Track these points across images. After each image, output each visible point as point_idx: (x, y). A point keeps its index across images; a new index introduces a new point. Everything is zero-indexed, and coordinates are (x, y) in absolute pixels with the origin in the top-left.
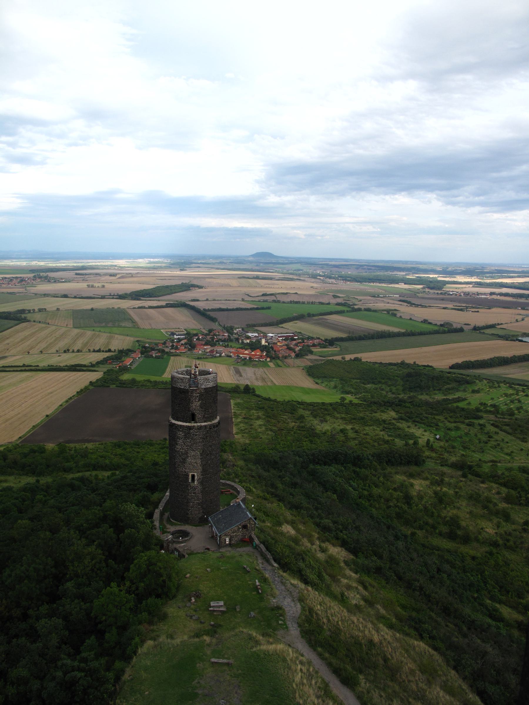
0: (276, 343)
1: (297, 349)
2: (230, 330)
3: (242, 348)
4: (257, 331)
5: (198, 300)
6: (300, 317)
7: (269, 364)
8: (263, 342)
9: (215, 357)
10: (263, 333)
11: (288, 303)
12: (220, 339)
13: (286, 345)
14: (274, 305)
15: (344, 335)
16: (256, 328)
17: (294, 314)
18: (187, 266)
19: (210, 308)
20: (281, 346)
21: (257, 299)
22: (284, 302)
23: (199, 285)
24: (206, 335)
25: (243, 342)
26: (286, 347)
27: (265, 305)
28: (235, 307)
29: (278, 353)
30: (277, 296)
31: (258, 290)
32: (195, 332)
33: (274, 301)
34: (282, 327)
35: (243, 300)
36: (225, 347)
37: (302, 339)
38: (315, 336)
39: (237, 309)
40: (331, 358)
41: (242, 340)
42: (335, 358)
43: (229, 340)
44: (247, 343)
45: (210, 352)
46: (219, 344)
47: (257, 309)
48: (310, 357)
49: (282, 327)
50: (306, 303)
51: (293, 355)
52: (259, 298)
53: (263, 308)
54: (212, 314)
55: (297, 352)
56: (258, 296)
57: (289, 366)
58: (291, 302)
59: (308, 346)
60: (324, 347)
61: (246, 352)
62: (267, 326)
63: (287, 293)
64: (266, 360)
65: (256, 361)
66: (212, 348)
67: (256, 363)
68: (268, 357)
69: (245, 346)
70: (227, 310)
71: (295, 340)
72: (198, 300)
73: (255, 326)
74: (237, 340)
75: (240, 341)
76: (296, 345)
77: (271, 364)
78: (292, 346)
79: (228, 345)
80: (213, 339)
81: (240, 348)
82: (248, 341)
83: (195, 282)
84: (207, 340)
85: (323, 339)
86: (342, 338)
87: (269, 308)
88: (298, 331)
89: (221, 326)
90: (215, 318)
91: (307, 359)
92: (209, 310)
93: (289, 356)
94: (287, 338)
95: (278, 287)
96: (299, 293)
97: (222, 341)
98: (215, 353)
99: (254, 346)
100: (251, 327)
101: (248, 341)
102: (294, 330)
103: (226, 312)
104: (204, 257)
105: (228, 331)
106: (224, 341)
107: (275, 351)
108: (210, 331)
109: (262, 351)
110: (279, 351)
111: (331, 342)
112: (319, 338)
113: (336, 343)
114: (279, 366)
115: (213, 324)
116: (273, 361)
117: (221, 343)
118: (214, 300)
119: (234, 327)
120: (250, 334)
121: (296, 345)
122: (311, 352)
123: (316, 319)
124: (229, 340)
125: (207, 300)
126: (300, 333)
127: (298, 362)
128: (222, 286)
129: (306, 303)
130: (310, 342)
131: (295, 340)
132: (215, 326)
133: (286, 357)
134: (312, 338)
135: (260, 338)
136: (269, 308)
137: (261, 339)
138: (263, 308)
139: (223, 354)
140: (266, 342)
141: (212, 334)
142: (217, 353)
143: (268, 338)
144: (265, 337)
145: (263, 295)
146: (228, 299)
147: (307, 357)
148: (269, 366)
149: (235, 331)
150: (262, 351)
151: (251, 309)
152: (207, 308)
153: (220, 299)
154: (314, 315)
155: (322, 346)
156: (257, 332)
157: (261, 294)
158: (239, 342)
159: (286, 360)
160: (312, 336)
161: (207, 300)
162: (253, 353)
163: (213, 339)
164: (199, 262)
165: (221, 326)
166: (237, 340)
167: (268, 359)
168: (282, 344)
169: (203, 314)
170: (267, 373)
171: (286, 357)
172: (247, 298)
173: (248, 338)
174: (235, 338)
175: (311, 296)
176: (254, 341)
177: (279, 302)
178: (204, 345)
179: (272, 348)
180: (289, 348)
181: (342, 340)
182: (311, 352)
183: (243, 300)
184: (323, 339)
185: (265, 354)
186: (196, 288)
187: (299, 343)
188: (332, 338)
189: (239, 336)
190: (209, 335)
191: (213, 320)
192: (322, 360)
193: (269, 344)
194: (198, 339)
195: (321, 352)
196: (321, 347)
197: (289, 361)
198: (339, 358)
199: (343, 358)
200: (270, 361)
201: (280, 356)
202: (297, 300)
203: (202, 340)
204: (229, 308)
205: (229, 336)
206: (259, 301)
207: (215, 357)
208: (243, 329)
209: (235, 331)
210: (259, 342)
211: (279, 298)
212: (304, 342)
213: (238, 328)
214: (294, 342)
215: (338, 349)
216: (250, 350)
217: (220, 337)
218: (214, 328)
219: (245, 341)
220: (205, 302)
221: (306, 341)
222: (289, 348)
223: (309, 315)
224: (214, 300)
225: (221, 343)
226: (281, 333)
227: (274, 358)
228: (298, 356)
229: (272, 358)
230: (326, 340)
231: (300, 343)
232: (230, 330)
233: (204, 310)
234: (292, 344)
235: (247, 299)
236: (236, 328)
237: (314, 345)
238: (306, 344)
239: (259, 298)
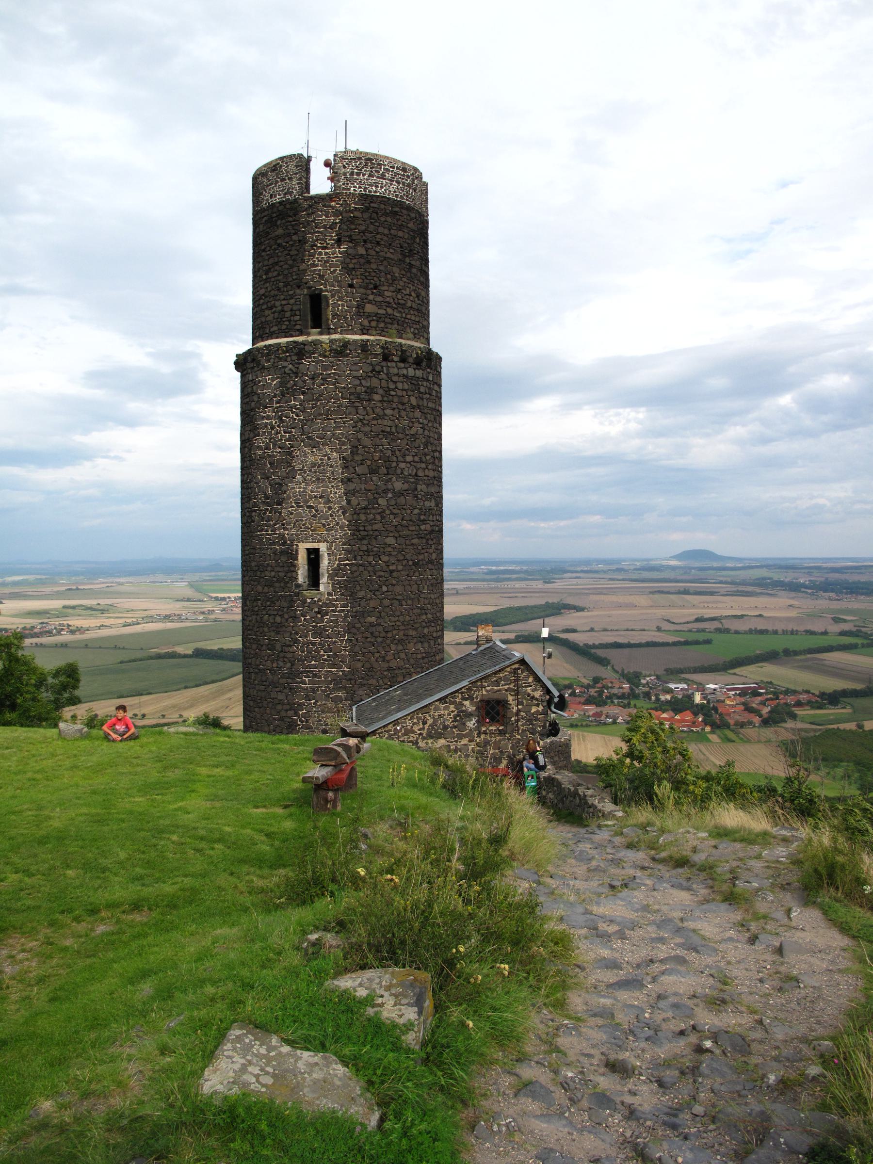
1: (765, 711)
2: (634, 678)
3: (656, 709)
4: (685, 681)
5: (574, 631)
6: (770, 657)
7: (709, 736)
8: (698, 698)
9: (605, 724)
10: (696, 683)
12: (614, 695)
13: (743, 704)
14: (717, 638)
15: (858, 686)
16: (683, 676)
17: (758, 652)
18: (556, 576)
19: (597, 643)
20: (733, 706)
21: (685, 627)
22: (737, 632)
23: (577, 604)
24: (588, 687)
25: (658, 699)
26: (742, 707)
27: (701, 637)
28: (644, 641)
29: (726, 718)
30: (723, 621)
31: (686, 611)
32: (567, 682)
33: (718, 631)
34: (735, 674)
35: (659, 629)
36: (624, 707)
37: (774, 693)
38: (799, 689)
39: (649, 644)
40: (835, 726)
41: (657, 696)
42: (842, 726)
43: (633, 695)
44: (667, 702)
45: (594, 715)
46: (612, 702)
47: (686, 643)
48: (790, 724)
49: (735, 674)
50: (780, 632)
51: (757, 720)
52: (690, 626)
53: (697, 643)
54: (600, 653)
55: (766, 716)
56: (688, 623)
57: (748, 741)
58: (750, 631)
59: (786, 704)
60: (820, 708)
61: (665, 715)
62: (706, 672)
63: (742, 616)
64: (703, 729)
65: (682, 731)
66: (599, 709)
67: (684, 735)
68: (706, 724)
69: (661, 706)
70: (629, 646)
71: (760, 694)
72: (574, 631)
73: (681, 671)
74: (647, 695)
75: (653, 698)
76: (763, 703)
77: (714, 738)
78: (754, 705)
79: (629, 704)
80: (600, 693)
81: (651, 709)
82: (668, 697)
83: (570, 601)
84: (590, 696)
85: (817, 693)
86: (855, 690)
87: (708, 642)
88: (765, 680)
89: (617, 672)
90: (606, 659)
91: (786, 729)
92: (594, 646)
93: (750, 723)
94: (743, 692)
95: (725, 607)
96: (765, 615)
97: (619, 698)
98: (603, 718)
99: (681, 705)
100: (675, 673)
101: (668, 697)
102: (758, 678)
103: (626, 651)
104: (588, 562)
105: (629, 681)
106: (622, 696)
107: (721, 715)
108: (596, 680)
109: (695, 714)
110: (729, 714)
111: (833, 698)
112: (808, 692)
113: (845, 700)
114: (730, 741)
115: (602, 669)
116: (718, 731)
117: (616, 701)
118: (605, 630)
119: (641, 673)
120: (672, 686)
121: (763, 703)
122: (794, 717)
123: (801, 660)
124: (633, 695)
125: (592, 630)
126: (771, 683)
127: (768, 732)
128: (620, 606)
129: (780, 632)
131: (760, 694)
132: (606, 673)
133: (742, 725)
134: (795, 692)
135: (690, 692)
136: (708, 642)
137: (693, 693)
138: (697, 643)
139: (620, 720)
140: (704, 698)
141: (599, 685)
142: (607, 717)
144: (701, 688)
145: (698, 620)
146: (630, 628)
147: (783, 725)
148: (708, 740)
149: (643, 681)
150: (695, 714)
151: (675, 644)
152: (590, 643)
153: (615, 628)
154: (796, 653)
155: (816, 705)
157: (693, 618)
158: (650, 699)
159: (742, 731)
160: (793, 688)
161: (592, 630)
162: (678, 717)
163: (600, 693)
164: (579, 569)
165: (617, 672)
166: (647, 695)
167: (708, 729)
168: (734, 703)
169: (584, 652)
170: (707, 753)
171: (742, 725)
172: (666, 626)
173: (669, 691)
174: (643, 693)
175: (789, 619)
176: (680, 697)
177: (727, 631)
178: (584, 704)
179: (715, 709)
180: (748, 709)
181: (855, 694)
182: (794, 717)
183: (659, 629)
184: (817, 693)
185: (700, 719)
186: (571, 611)
187: (767, 700)
188: (835, 691)
189: (651, 688)
190: (594, 687)
191: (603, 662)
192: (815, 731)
193: (708, 702)
194: (573, 694)
195: (814, 716)
196: (813, 708)
197: (748, 731)
198: (852, 726)
199: (860, 726)
200: (712, 732)
201: (732, 722)
202: (764, 628)
203: (579, 696)
204: (632, 642)
205: (631, 689)
206: (690, 631)
207: (605, 724)
208: (658, 678)
209: (643, 681)
210: (690, 697)
211: (727, 624)
212: (777, 698)
213: (649, 676)
214: (759, 698)
215: (848, 710)
216: (671, 713)
217: (615, 691)
218: (604, 677)
219: (662, 698)
220: (589, 634)
221: (781, 696)
222: (748, 709)
223: (787, 653)
224: (605, 630)
225: (616, 701)
226: (733, 684)
227: (719, 727)
228: (766, 722)
229: (715, 726)
230: (822, 695)
231: (771, 699)
232: (634, 678)
233: (586, 645)
234: (755, 703)
235: (667, 628)
236: (645, 677)
237: (799, 704)
238: (782, 702)
239: (690, 626)
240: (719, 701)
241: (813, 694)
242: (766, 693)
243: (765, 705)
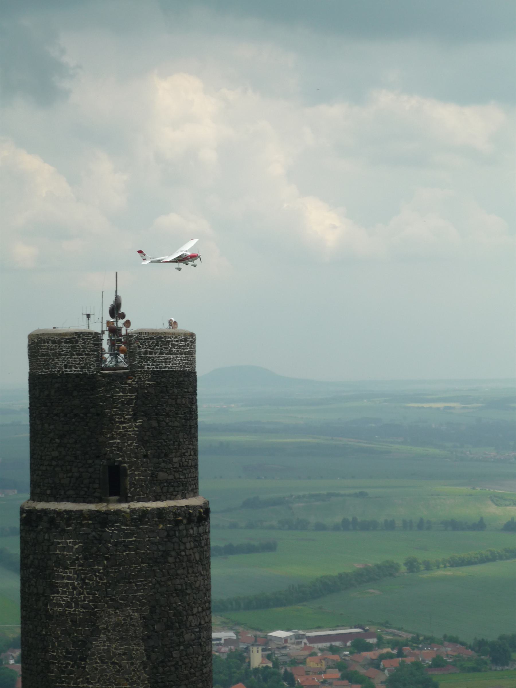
0: (303, 662)
8: (257, 659)
11: (336, 528)
26: (336, 674)
37: (395, 644)
59: (417, 665)
112: (453, 641)
130: (426, 656)
131: (369, 647)
134: (430, 641)
135: (242, 646)
137: (247, 650)
143: (272, 646)
156: (231, 629)
187: (382, 657)
193: (276, 665)
212: (400, 654)
214: (369, 655)
221: (407, 650)
230: (480, 646)
231: (390, 656)
238: (409, 660)
240: (294, 662)
241: (462, 644)
242: (381, 644)
243: (377, 667)
